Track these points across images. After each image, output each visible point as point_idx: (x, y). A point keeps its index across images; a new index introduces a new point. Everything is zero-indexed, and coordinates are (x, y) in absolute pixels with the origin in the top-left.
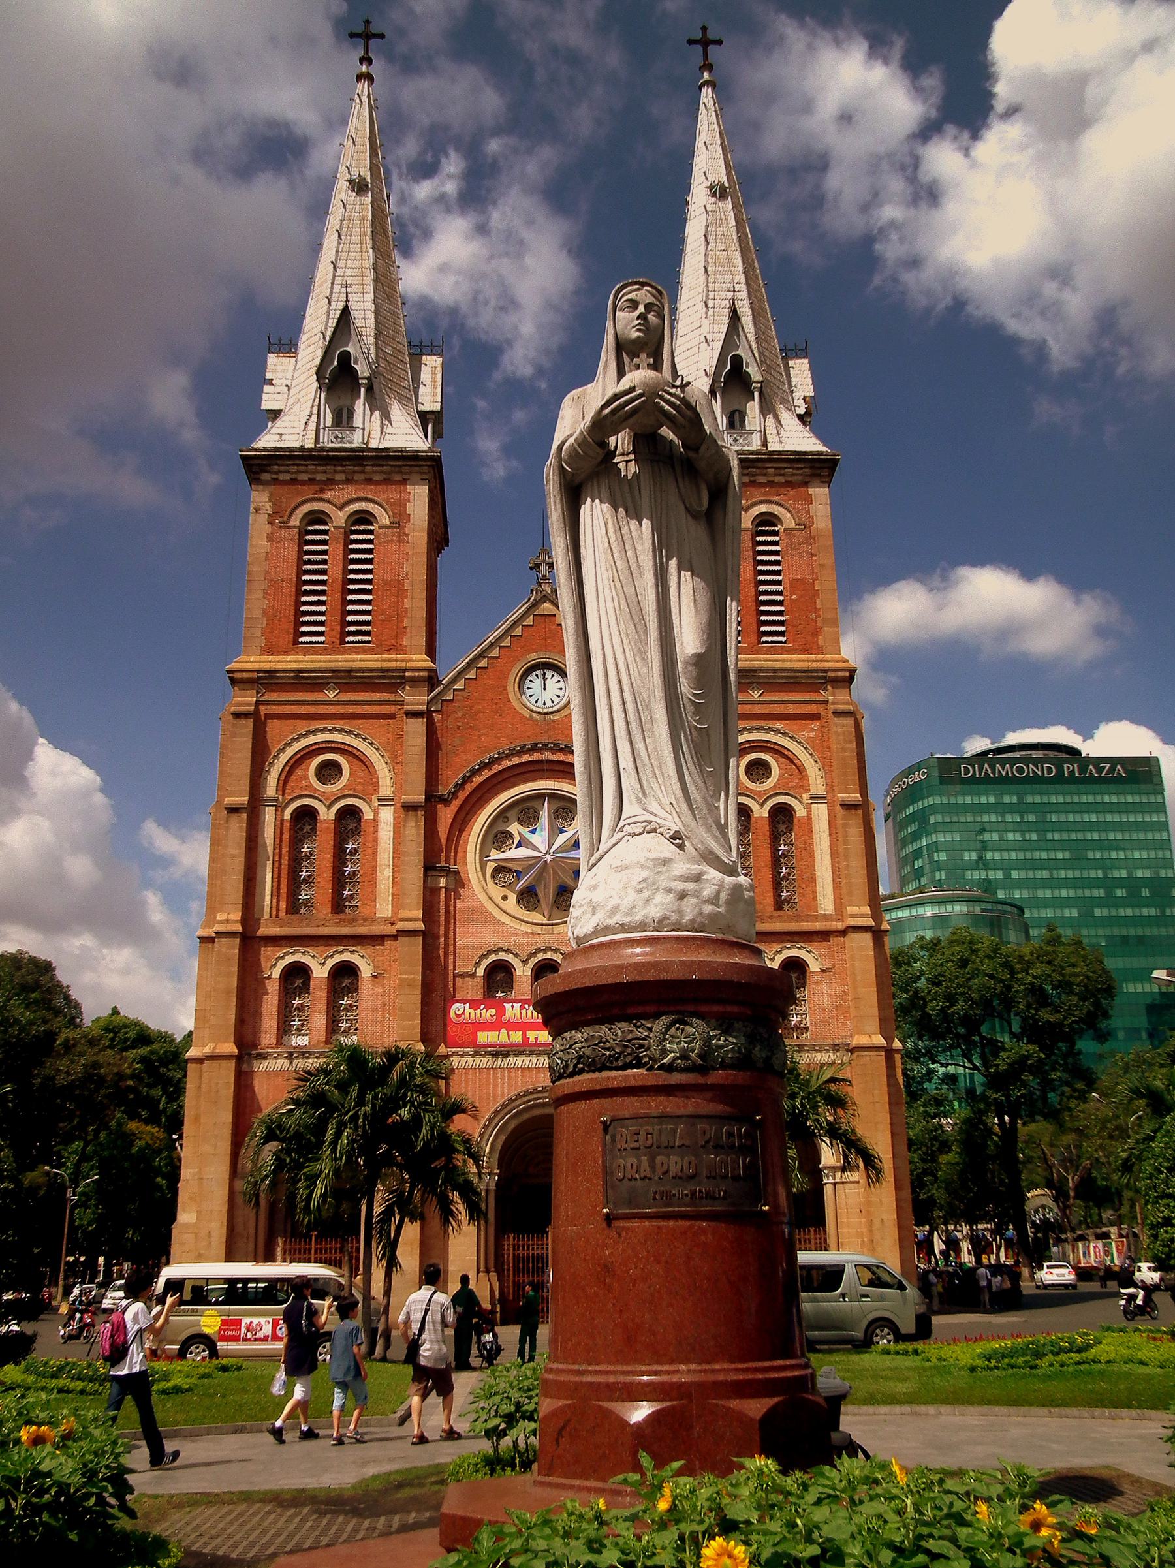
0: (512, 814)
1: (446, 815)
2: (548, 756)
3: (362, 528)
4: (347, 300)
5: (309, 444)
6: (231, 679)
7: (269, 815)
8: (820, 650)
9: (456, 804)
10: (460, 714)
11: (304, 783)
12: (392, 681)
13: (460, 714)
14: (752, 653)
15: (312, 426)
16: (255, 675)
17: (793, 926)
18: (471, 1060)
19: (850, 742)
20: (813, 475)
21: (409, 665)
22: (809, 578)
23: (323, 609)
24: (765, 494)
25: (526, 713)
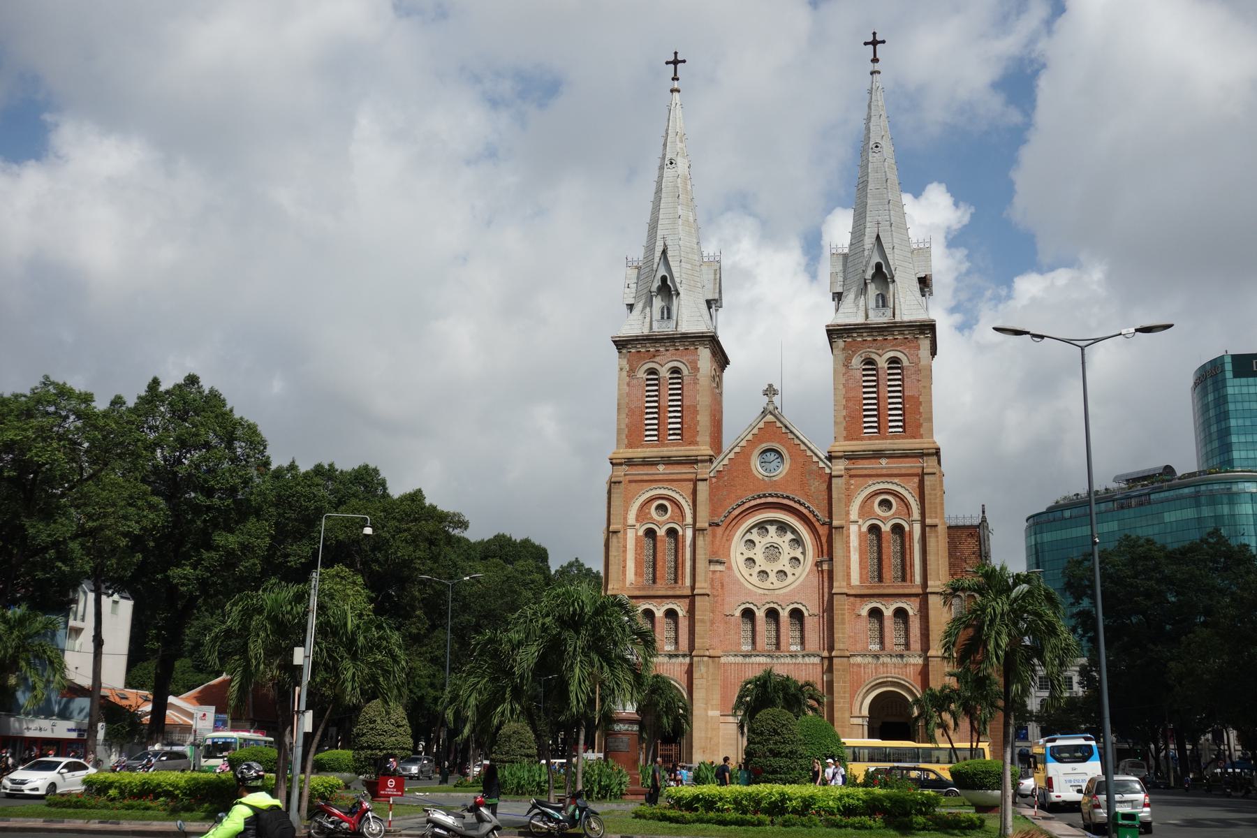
0: (755, 531)
1: (719, 531)
2: (770, 500)
3: (675, 375)
4: (665, 244)
5: (646, 332)
6: (611, 463)
7: (631, 534)
8: (921, 436)
9: (724, 525)
10: (726, 478)
11: (649, 516)
12: (692, 461)
13: (726, 478)
14: (883, 439)
15: (648, 319)
16: (623, 461)
17: (901, 591)
18: (733, 658)
19: (934, 490)
20: (920, 334)
21: (700, 453)
22: (916, 395)
23: (656, 422)
24: (893, 346)
25: (760, 477)
